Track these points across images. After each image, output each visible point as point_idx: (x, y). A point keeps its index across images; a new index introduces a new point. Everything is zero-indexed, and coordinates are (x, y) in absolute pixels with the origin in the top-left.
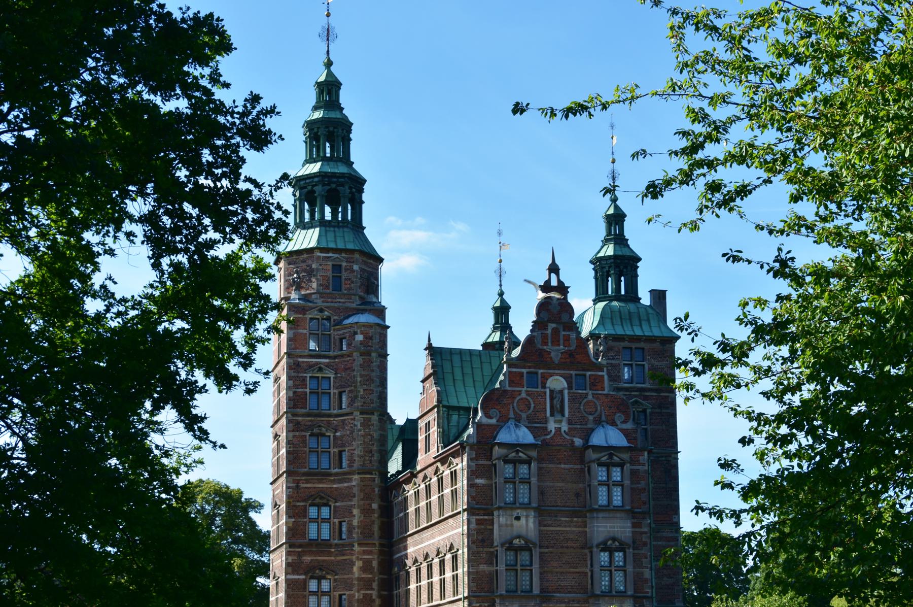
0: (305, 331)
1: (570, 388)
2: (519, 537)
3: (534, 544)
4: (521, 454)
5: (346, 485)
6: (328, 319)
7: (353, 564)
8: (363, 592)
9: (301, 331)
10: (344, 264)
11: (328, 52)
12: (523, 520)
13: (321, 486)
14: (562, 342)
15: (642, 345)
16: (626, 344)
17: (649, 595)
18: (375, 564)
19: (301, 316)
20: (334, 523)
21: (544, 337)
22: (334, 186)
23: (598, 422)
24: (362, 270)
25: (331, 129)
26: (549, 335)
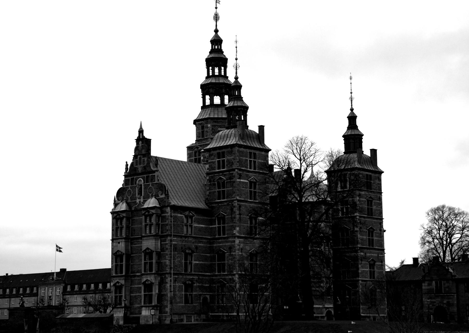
1: (144, 183)
2: (118, 251)
3: (124, 254)
9: (191, 158)
11: (216, 25)
12: (121, 243)
15: (223, 150)
16: (218, 151)
17: (168, 272)
21: (137, 161)
23: (152, 196)
24: (213, 126)
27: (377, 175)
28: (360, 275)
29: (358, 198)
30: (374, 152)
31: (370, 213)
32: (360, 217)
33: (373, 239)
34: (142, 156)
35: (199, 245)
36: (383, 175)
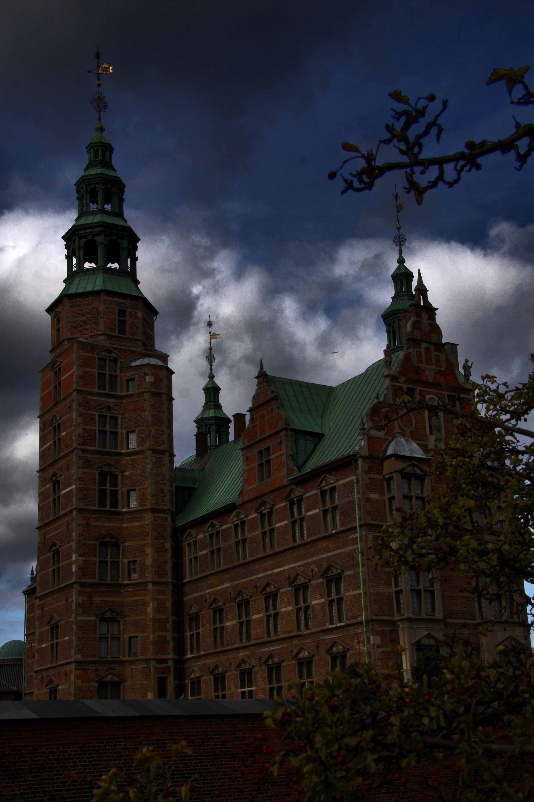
0: (93, 370)
4: (416, 469)
5: (136, 524)
6: (115, 361)
7: (146, 604)
8: (158, 633)
10: (129, 310)
13: (110, 525)
14: (434, 362)
18: (169, 604)
19: (90, 355)
20: (123, 563)
22: (114, 237)
25: (109, 186)
26: (423, 353)
34: (432, 347)
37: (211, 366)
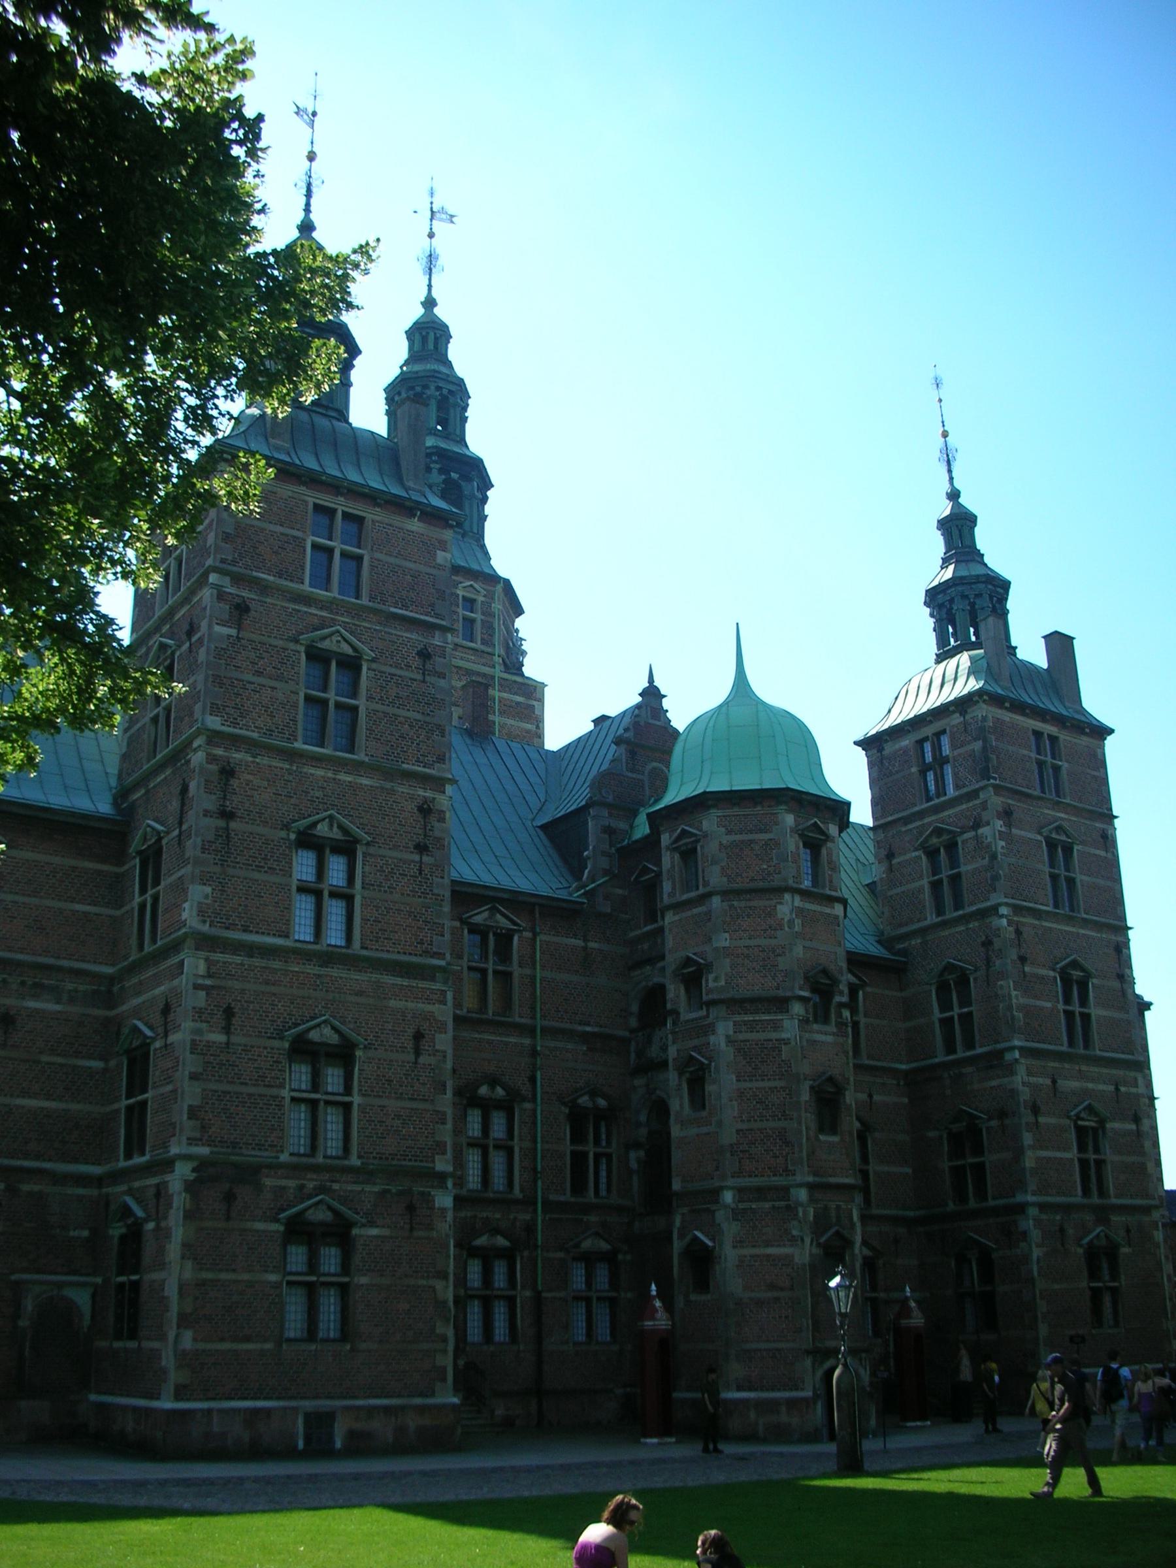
11: (430, 286)
27: (1085, 740)
28: (1032, 1186)
29: (999, 824)
30: (1060, 645)
31: (1064, 889)
32: (1017, 910)
33: (1086, 1017)
35: (32, 1004)
36: (1110, 742)
37: (950, 471)
